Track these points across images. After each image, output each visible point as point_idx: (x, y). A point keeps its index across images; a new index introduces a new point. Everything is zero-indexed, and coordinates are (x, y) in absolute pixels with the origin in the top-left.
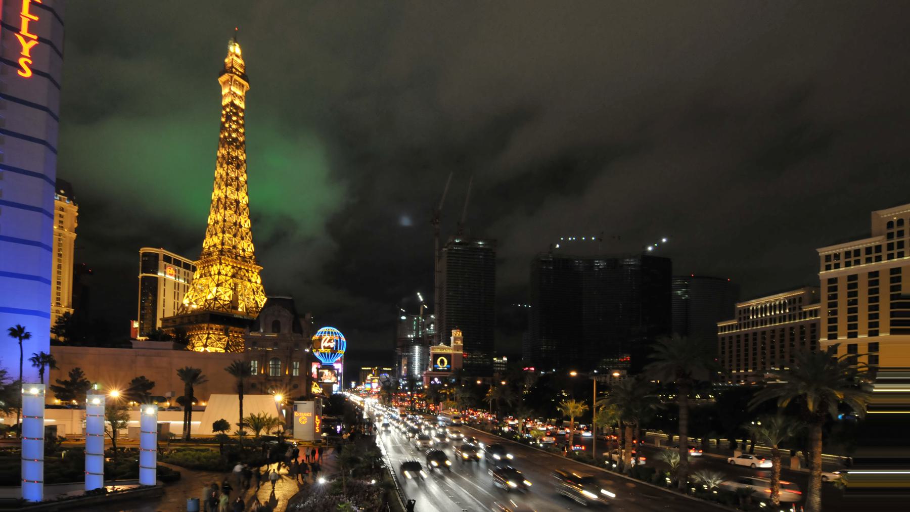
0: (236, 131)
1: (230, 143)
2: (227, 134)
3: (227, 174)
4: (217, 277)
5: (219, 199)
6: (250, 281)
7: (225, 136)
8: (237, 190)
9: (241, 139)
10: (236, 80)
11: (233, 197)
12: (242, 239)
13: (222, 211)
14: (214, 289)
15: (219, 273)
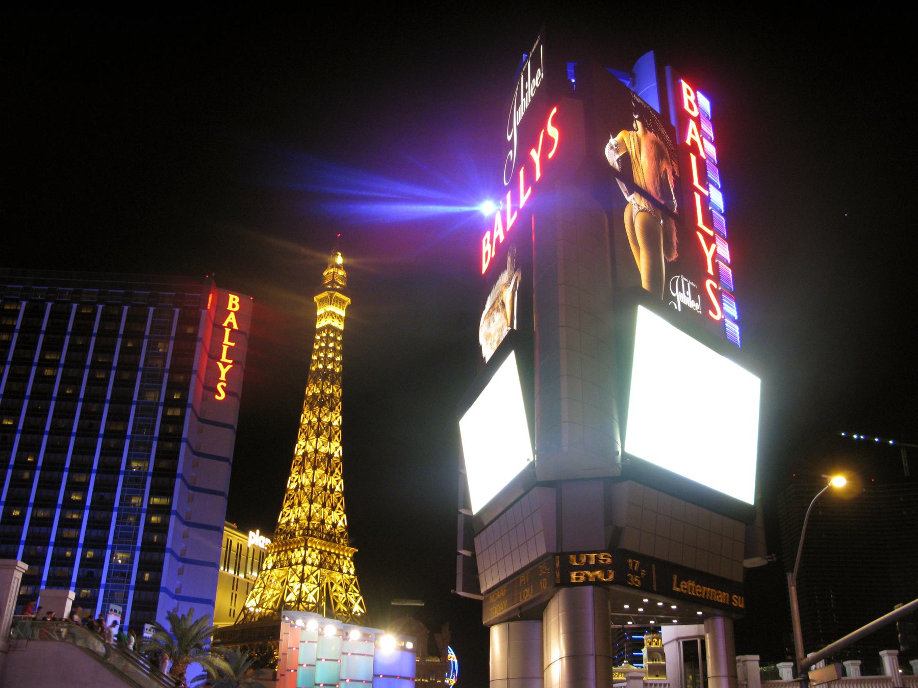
0: (333, 360)
1: (325, 378)
2: (321, 366)
3: (319, 420)
4: (300, 568)
5: (305, 454)
6: (341, 571)
7: (317, 369)
8: (330, 440)
9: (338, 370)
10: (337, 297)
11: (323, 450)
12: (333, 508)
13: (309, 471)
14: (296, 586)
15: (304, 563)
